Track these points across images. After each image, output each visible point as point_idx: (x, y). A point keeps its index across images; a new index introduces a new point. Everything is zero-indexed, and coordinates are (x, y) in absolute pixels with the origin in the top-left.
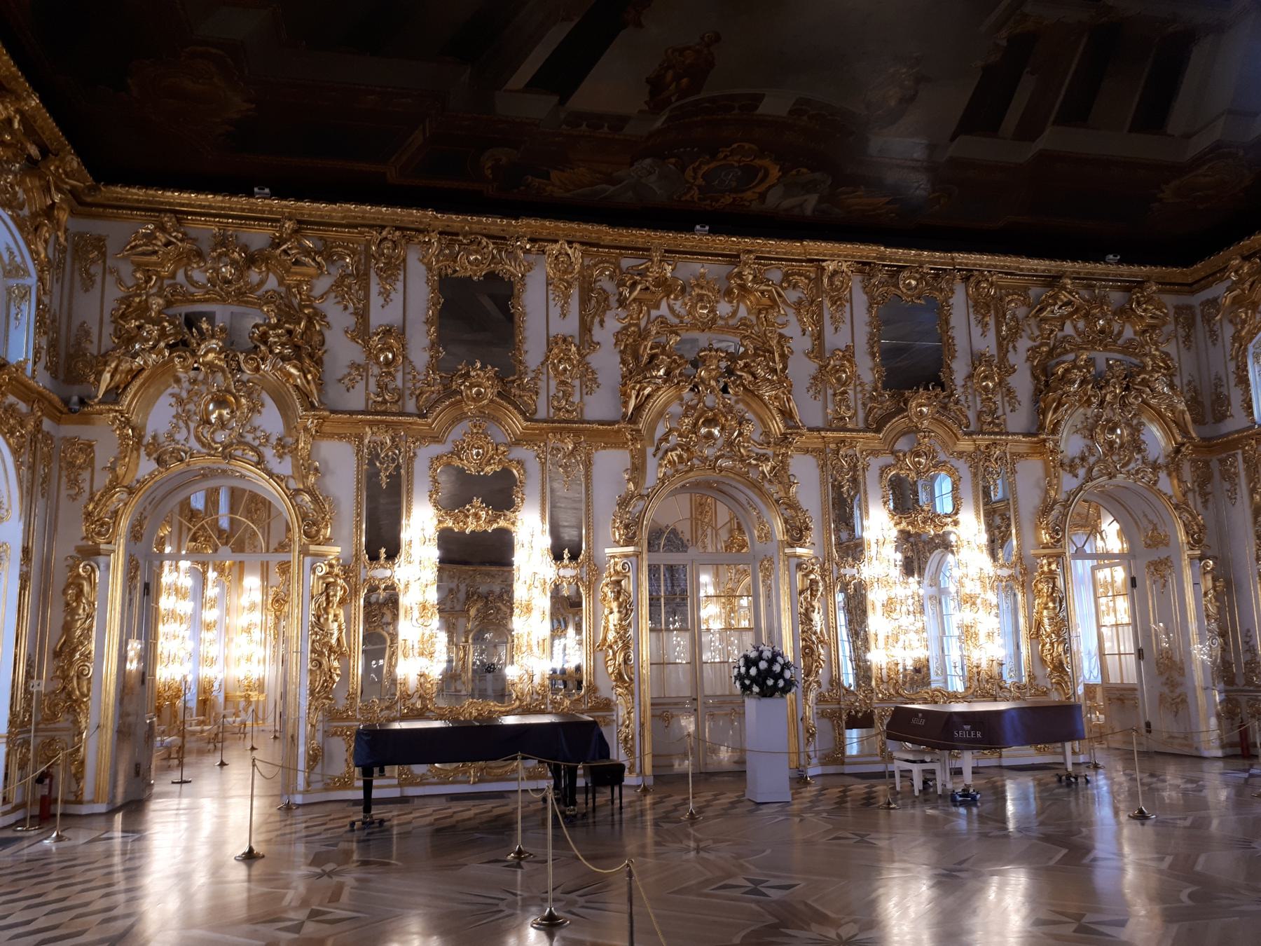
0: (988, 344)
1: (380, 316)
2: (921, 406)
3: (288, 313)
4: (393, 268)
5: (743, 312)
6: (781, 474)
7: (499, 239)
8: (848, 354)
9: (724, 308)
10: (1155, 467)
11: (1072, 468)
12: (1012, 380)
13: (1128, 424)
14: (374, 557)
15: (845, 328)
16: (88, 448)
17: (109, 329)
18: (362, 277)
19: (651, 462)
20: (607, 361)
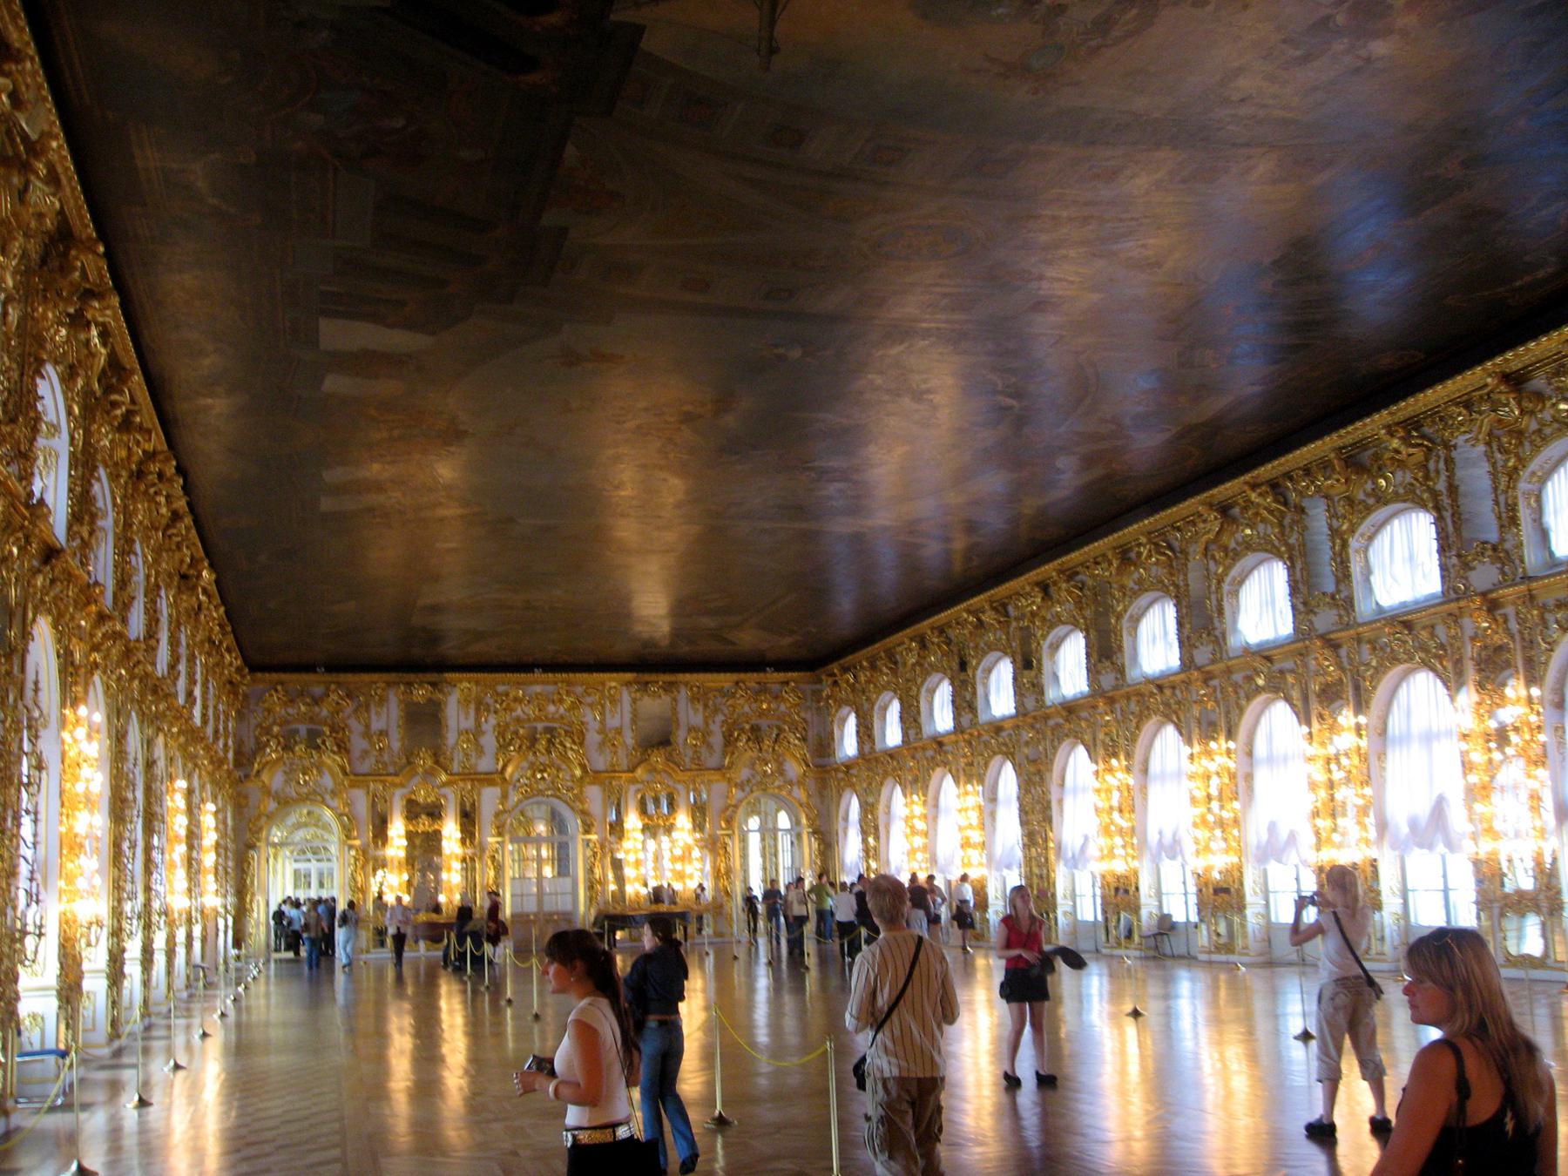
0: (697, 719)
1: (377, 724)
2: (658, 758)
3: (333, 730)
4: (382, 701)
5: (562, 710)
6: (580, 798)
7: (433, 684)
8: (619, 731)
9: (552, 708)
10: (791, 783)
11: (741, 786)
12: (712, 740)
13: (776, 760)
14: (376, 844)
15: (618, 716)
16: (246, 797)
17: (252, 740)
18: (368, 710)
19: (511, 792)
20: (489, 741)
